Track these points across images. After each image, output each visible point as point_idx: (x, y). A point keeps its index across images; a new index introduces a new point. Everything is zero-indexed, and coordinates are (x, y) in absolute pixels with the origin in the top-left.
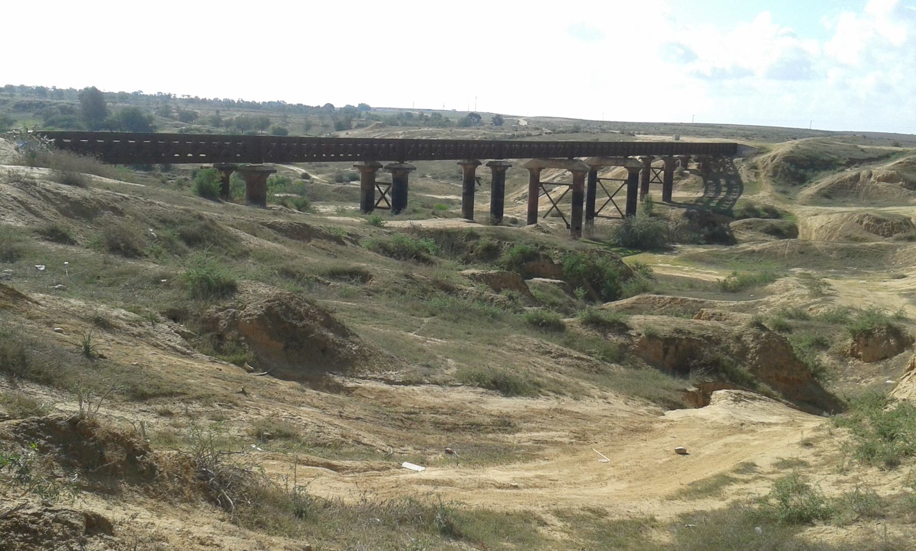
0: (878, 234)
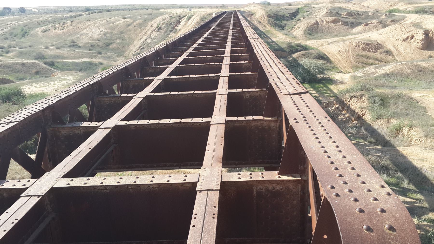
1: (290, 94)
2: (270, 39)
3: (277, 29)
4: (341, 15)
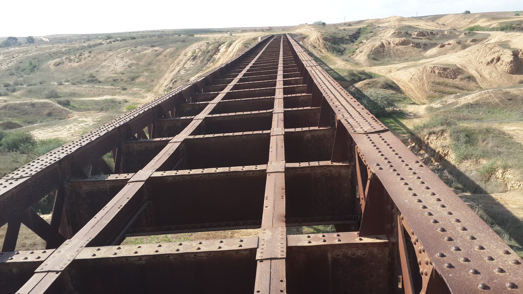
0: (448, 78)
1: (366, 133)
2: (327, 66)
3: (335, 54)
4: (411, 35)
